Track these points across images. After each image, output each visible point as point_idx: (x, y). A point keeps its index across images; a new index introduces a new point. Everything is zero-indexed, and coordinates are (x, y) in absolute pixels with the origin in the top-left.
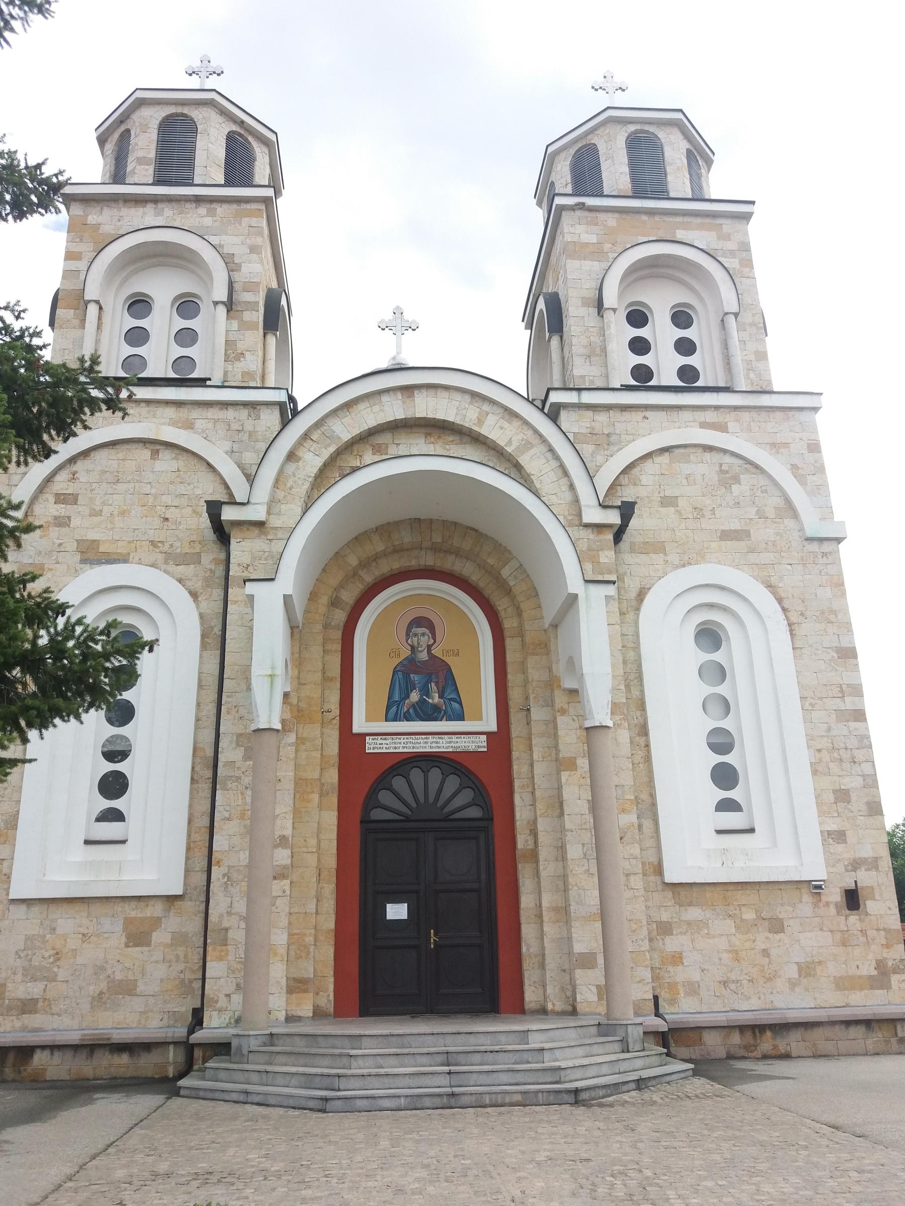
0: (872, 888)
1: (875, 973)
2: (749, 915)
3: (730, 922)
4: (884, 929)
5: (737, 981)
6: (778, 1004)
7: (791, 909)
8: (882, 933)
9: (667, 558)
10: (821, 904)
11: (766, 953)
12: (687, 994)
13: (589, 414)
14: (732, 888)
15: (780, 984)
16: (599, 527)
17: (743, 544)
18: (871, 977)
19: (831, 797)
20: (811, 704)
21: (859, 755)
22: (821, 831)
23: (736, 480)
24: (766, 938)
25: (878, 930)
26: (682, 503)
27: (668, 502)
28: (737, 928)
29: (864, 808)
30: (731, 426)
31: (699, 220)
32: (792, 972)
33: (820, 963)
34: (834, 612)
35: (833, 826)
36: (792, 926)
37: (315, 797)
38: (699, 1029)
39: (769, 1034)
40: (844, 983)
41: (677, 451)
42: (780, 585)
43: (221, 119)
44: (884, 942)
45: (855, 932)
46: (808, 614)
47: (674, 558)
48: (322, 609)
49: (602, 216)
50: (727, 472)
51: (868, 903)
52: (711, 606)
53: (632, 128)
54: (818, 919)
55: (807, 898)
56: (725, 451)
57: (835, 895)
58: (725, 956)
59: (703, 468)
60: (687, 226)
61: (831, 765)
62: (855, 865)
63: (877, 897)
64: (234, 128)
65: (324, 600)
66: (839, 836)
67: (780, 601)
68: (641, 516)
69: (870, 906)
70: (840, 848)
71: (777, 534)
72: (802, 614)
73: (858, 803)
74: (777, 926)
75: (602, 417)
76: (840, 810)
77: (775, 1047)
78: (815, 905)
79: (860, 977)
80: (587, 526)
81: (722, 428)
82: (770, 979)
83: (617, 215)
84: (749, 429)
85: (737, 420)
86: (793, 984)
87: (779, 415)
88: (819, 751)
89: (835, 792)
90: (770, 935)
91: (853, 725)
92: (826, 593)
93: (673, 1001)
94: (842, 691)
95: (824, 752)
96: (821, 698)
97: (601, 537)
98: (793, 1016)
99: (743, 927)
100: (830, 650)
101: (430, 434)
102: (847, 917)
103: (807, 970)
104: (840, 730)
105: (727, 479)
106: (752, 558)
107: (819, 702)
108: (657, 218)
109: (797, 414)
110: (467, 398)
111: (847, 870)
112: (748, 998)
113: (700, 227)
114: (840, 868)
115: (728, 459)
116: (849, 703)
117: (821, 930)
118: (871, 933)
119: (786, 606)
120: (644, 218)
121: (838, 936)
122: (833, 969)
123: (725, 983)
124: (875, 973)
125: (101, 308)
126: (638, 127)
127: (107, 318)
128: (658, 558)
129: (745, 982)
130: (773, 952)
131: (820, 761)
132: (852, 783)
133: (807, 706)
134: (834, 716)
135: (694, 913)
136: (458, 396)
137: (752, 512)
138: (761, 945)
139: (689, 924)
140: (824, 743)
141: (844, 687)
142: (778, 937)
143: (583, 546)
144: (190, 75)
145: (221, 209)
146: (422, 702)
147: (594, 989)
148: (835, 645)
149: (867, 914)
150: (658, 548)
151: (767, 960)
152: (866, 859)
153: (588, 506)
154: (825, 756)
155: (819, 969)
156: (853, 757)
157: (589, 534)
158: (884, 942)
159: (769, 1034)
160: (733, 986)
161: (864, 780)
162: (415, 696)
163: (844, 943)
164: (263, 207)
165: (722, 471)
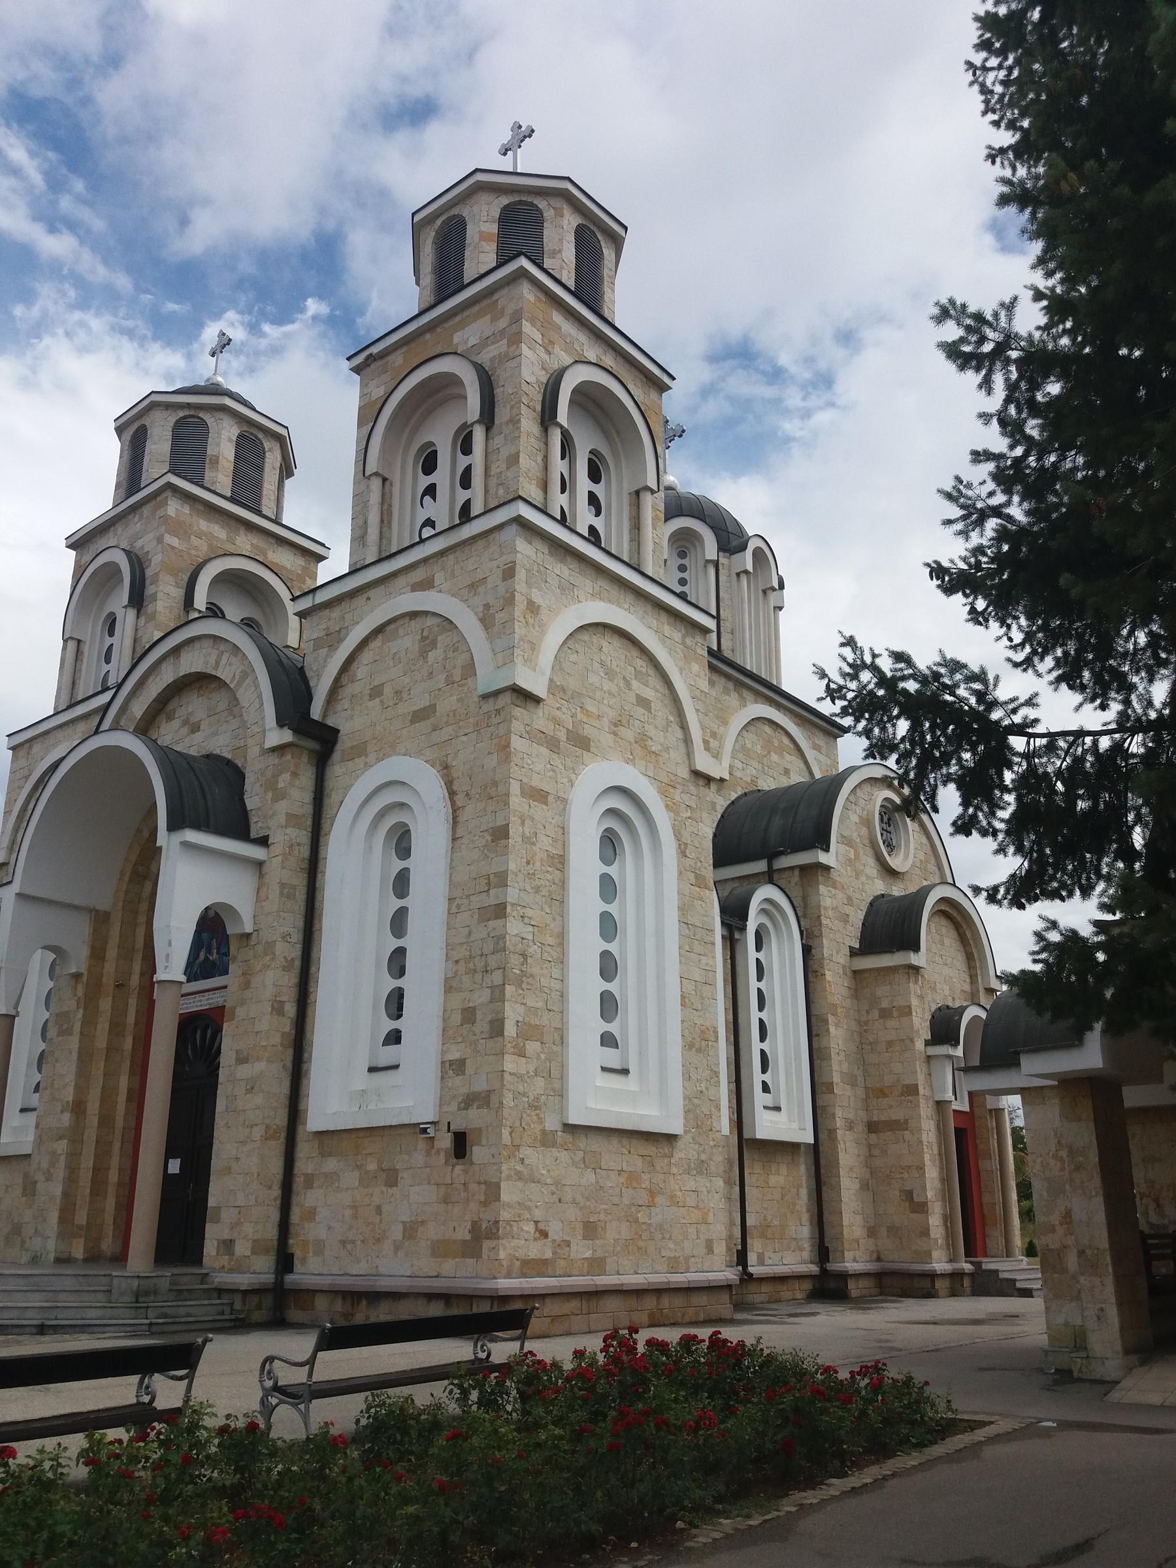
0: (480, 1130)
1: (468, 1237)
2: (372, 1166)
3: (356, 1174)
4: (485, 1183)
5: (353, 1242)
6: (382, 1270)
7: (407, 1157)
8: (483, 1186)
9: (368, 760)
10: (433, 1151)
11: (379, 1210)
12: (316, 1253)
13: (327, 612)
14: (362, 1134)
15: (387, 1246)
16: (280, 749)
17: (428, 722)
18: (464, 1241)
19: (457, 1018)
20: (458, 907)
21: (493, 961)
22: (443, 1062)
23: (434, 645)
24: (382, 1192)
25: (479, 1183)
26: (387, 690)
27: (376, 692)
28: (361, 1180)
29: (486, 1028)
30: (439, 578)
31: (476, 308)
32: (397, 1233)
33: (423, 1222)
34: (495, 784)
35: (454, 1055)
36: (405, 1177)
37: (102, 1064)
38: (312, 1292)
39: (364, 1302)
40: (441, 1249)
41: (388, 628)
42: (454, 763)
43: (165, 414)
44: (483, 1199)
45: (458, 1186)
46: (473, 792)
47: (371, 758)
48: (124, 887)
49: (390, 358)
50: (427, 637)
51: (475, 1149)
52: (402, 805)
53: (439, 222)
54: (428, 1170)
55: (422, 1145)
56: (426, 613)
57: (445, 1142)
58: (348, 1212)
59: (406, 641)
60: (462, 326)
61: (465, 979)
62: (470, 1101)
63: (484, 1142)
64: (181, 414)
65: (127, 878)
66: (457, 1067)
67: (449, 784)
68: (352, 718)
69: (478, 1153)
70: (458, 1080)
71: (460, 700)
72: (467, 795)
73: (482, 1025)
74: (392, 1178)
75: (336, 613)
76: (465, 1033)
77: (368, 1317)
78: (428, 1153)
79: (455, 1241)
80: (273, 750)
81: (426, 585)
82: (378, 1240)
83: (404, 349)
84: (453, 576)
85: (443, 569)
86: (397, 1247)
87: (481, 543)
88: (457, 962)
89: (464, 1010)
90: (384, 1189)
91: (492, 924)
92: (492, 761)
93: (304, 1260)
94: (488, 884)
95: (462, 963)
96: (468, 896)
97: (284, 759)
98: (384, 1284)
99: (367, 1180)
100: (486, 834)
101: (201, 687)
102: (453, 1166)
103: (411, 1230)
104: (480, 933)
105: (427, 644)
106: (436, 737)
107: (466, 901)
108: (439, 330)
109: (496, 534)
110: (211, 641)
111: (459, 1109)
112: (359, 1261)
113: (476, 317)
114: (454, 1107)
115: (430, 621)
116: (492, 899)
117: (429, 1183)
118: (473, 1187)
119: (455, 788)
120: (428, 336)
121: (443, 1189)
122: (433, 1232)
123: (343, 1243)
124: (468, 1237)
125: (79, 641)
126: (444, 217)
127: (86, 649)
128: (359, 761)
129: (359, 1242)
130: (385, 1208)
131: (456, 973)
132: (481, 997)
133: (454, 910)
134: (476, 916)
135: (332, 1164)
136: (207, 643)
137: (442, 678)
138: (376, 1200)
139: (326, 1175)
140: (462, 952)
141: (492, 876)
142: (390, 1191)
143: (269, 773)
144: (213, 356)
145: (146, 510)
146: (206, 958)
147: (215, 1243)
148: (491, 825)
149: (472, 1163)
150: (360, 750)
151: (378, 1218)
152: (479, 1093)
153: (270, 729)
154: (461, 967)
155: (420, 1229)
156: (486, 965)
157: (273, 759)
158: (483, 1199)
159: (364, 1302)
160: (349, 1247)
161: (492, 993)
162: (202, 955)
163: (446, 1200)
164: (168, 493)
165: (423, 639)
